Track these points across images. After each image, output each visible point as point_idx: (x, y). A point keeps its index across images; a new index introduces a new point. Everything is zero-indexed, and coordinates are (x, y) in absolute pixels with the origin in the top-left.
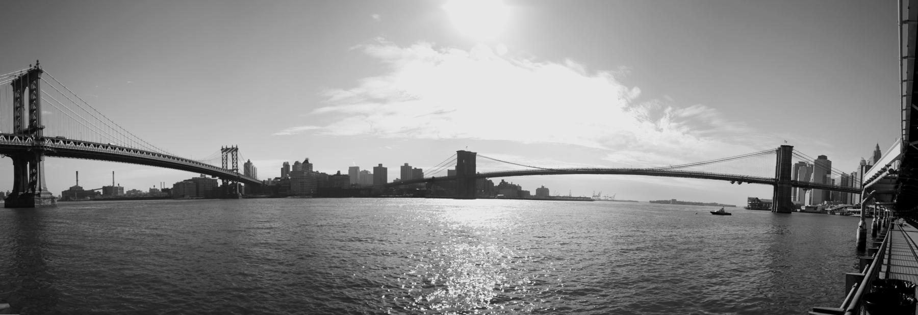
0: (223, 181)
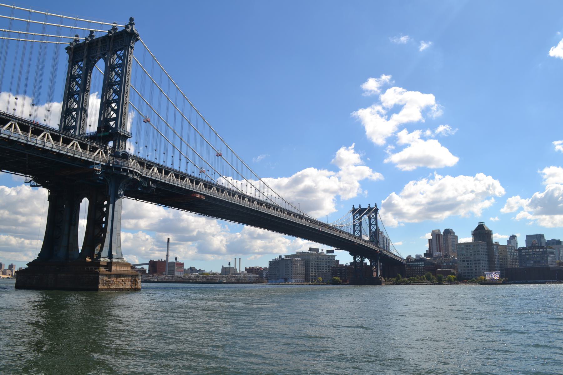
0: (355, 258)
